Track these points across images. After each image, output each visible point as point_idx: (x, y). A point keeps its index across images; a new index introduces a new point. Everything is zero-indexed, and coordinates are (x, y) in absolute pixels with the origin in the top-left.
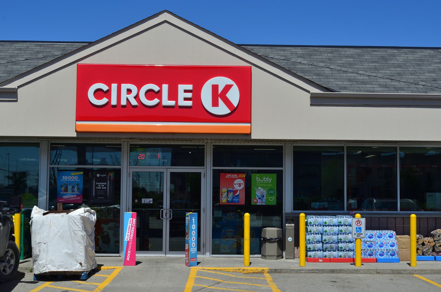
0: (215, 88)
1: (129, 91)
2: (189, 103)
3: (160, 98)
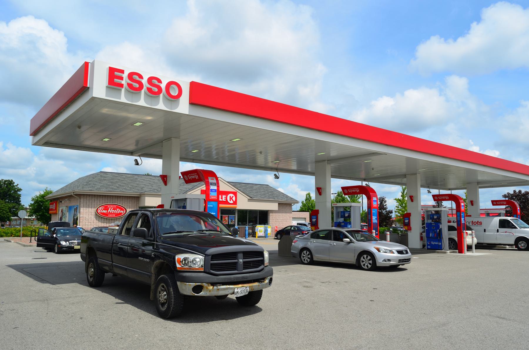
0: (230, 196)
2: (225, 200)
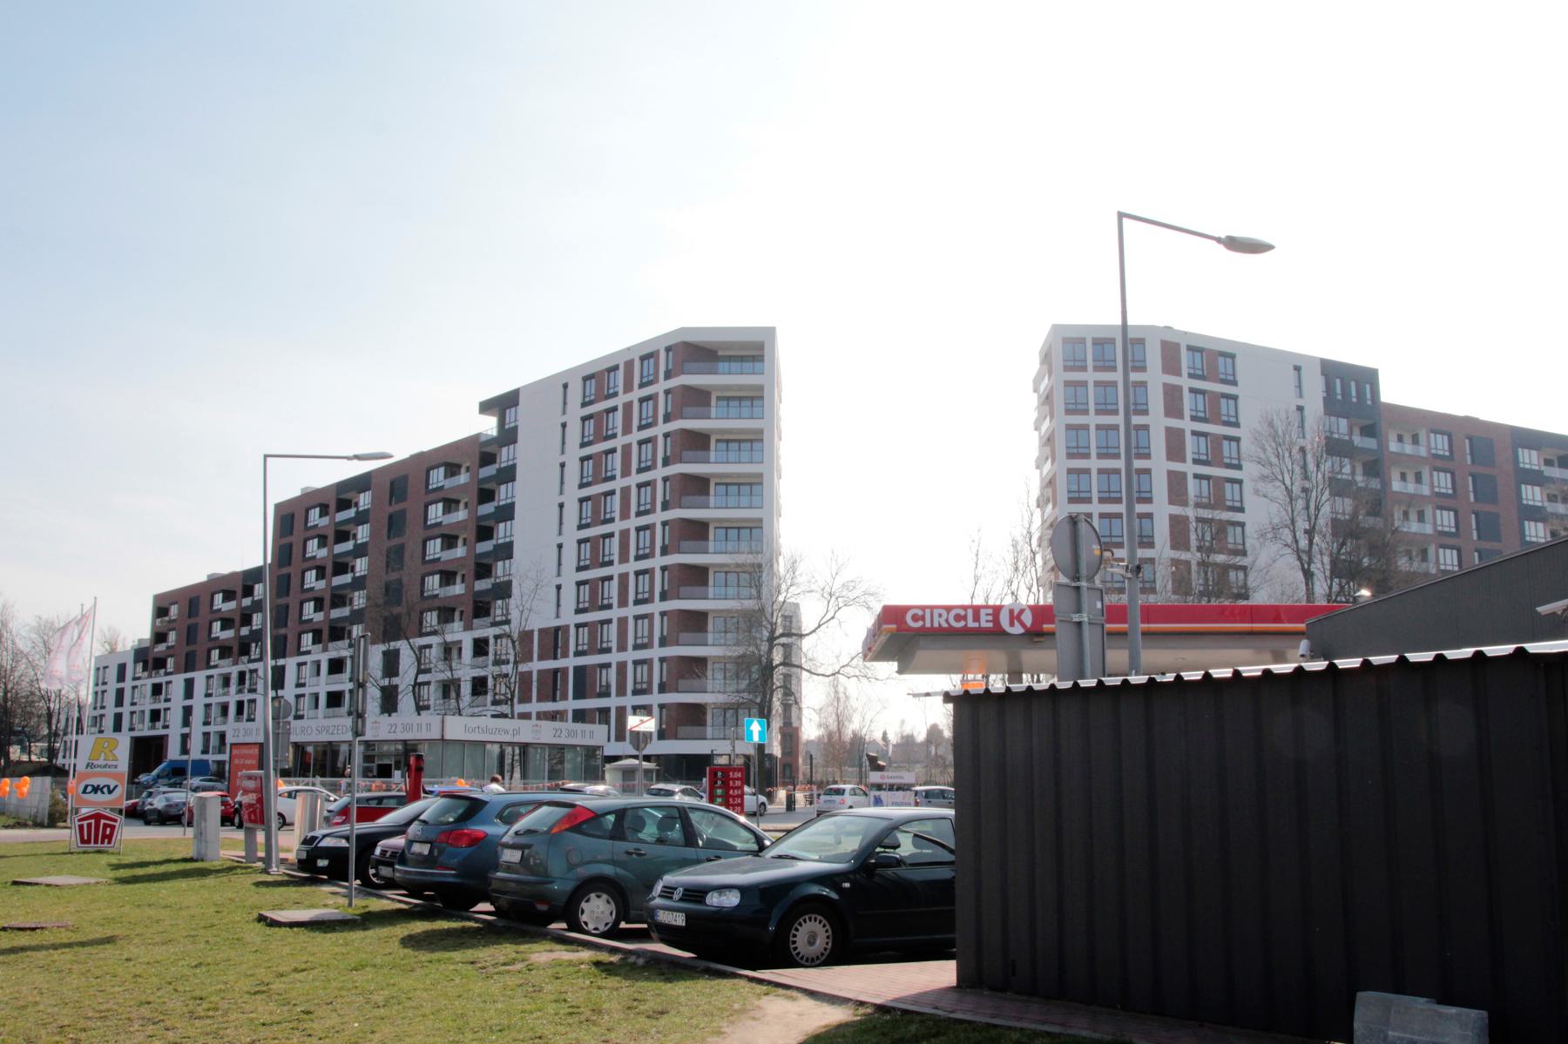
1: (940, 615)
2: (990, 625)
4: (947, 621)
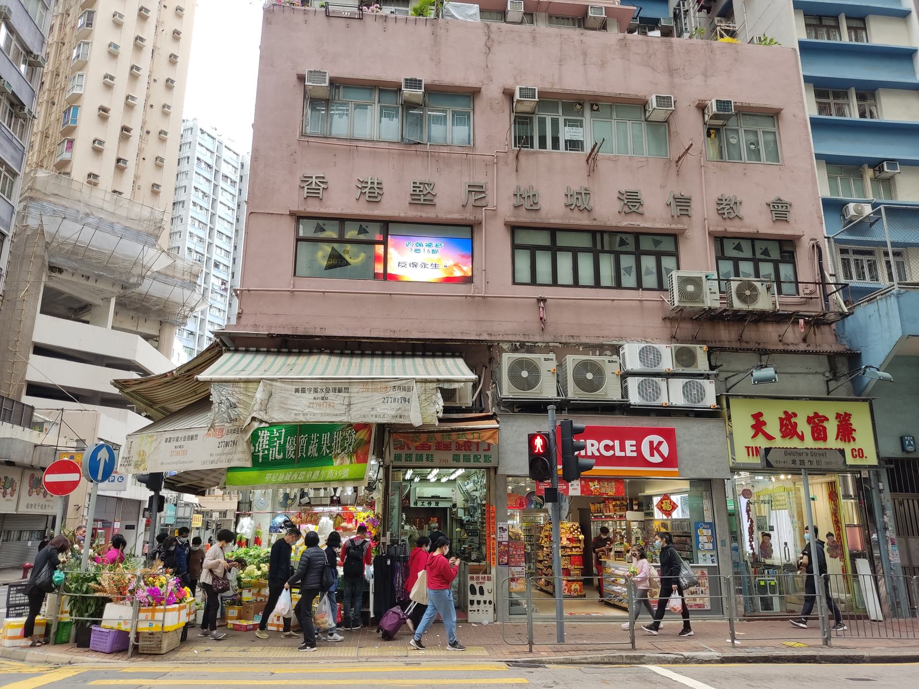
0: (651, 443)
1: (592, 445)
2: (635, 454)
3: (614, 450)
4: (598, 450)
